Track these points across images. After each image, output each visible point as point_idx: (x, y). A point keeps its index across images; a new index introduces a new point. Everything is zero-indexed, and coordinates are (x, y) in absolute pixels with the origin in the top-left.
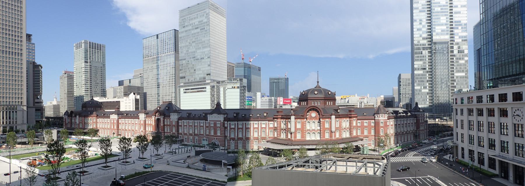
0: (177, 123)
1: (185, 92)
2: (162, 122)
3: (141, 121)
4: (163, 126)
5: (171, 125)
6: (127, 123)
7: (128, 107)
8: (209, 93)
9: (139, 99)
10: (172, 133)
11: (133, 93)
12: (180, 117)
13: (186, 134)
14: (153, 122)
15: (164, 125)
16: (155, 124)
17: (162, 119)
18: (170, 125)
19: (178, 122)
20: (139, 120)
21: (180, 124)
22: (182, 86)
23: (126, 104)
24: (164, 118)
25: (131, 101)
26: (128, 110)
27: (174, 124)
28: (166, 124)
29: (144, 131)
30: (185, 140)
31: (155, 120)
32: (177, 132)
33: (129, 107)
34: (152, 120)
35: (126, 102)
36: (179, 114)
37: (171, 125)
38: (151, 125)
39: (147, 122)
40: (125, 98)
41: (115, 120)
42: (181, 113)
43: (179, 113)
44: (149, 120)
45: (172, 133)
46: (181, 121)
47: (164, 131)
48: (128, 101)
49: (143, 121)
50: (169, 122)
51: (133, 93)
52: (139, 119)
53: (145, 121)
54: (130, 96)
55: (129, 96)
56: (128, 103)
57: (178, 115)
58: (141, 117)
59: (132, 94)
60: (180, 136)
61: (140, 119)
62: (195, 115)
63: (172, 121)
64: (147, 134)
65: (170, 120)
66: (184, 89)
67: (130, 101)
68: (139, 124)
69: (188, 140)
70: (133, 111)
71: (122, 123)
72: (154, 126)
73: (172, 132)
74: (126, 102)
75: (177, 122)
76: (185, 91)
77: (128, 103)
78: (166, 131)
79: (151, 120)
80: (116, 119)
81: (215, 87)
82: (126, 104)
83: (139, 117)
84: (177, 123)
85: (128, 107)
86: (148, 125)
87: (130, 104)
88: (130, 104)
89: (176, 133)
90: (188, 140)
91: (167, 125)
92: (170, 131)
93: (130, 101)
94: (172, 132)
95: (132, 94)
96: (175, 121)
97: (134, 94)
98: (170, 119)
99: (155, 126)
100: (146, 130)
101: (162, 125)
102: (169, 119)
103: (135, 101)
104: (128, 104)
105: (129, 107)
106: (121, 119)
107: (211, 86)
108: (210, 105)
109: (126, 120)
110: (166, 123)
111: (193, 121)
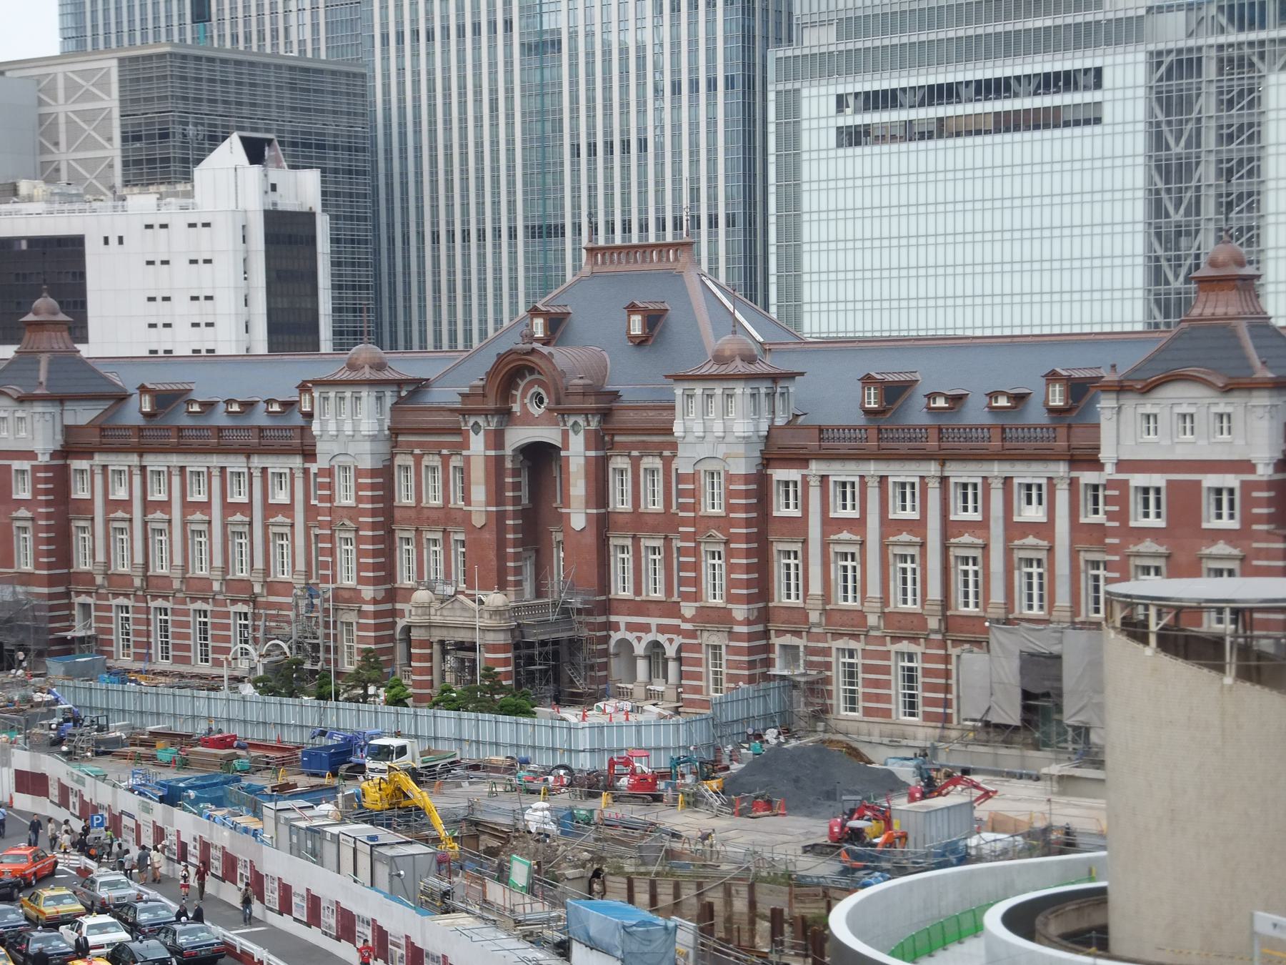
0: (747, 494)
1: (853, 137)
2: (578, 488)
3: (329, 472)
4: (590, 540)
5: (685, 521)
6: (165, 506)
7: (182, 311)
8: (1138, 143)
9: (311, 216)
10: (688, 609)
11: (235, 138)
12: (780, 422)
13: (851, 625)
14: (479, 493)
15: (603, 524)
16: (501, 516)
17: (577, 452)
18: (666, 524)
19: (760, 488)
20: (314, 468)
21: (781, 510)
22: (823, 65)
23: (159, 281)
24: (602, 442)
25: (222, 242)
26: (183, 342)
27: (712, 507)
28: (628, 507)
29: (368, 592)
30: (839, 687)
31: (499, 460)
32: (749, 599)
33: (201, 311)
34: (464, 471)
35: (158, 245)
36: (771, 396)
37: (685, 521)
38: (447, 519)
39: (404, 497)
40: (143, 202)
41: (16, 465)
42: (791, 376)
43: (774, 378)
44: (434, 461)
45: (688, 609)
46: (793, 474)
47: (604, 584)
48: (179, 242)
49: (359, 473)
50: (659, 488)
51: (235, 138)
52: (309, 454)
53: (384, 477)
54: (199, 173)
55: (187, 177)
56: (180, 264)
57: (764, 403)
58: (332, 428)
59: (231, 151)
60: (789, 640)
61: (320, 447)
62: (957, 400)
63: (693, 478)
64: (401, 623)
65: (667, 462)
66: (841, 101)
67: (203, 243)
68: (310, 511)
69: (876, 684)
70: (247, 358)
71: (111, 505)
72: (489, 536)
73: (696, 597)
74: (158, 245)
75: (747, 479)
76: (852, 119)
77: (180, 264)
78: (621, 590)
79: (456, 461)
80: (30, 455)
81: (1210, 70)
82: (159, 281)
83: (316, 427)
84: (747, 494)
85: (182, 311)
86: (421, 517)
87: (203, 279)
88: (203, 279)
89: (740, 611)
90: (876, 684)
91: (639, 523)
92: (669, 590)
93: (203, 243)
94: (696, 597)
95: (231, 151)
96: (730, 478)
97: (255, 152)
98: (674, 446)
99: (501, 529)
100: (391, 576)
101: (578, 520)
102: (657, 450)
103: (271, 239)
104: (181, 279)
105: (201, 311)
106: (99, 459)
107: (1156, 59)
108: (1137, 276)
109: (155, 462)
110: (620, 503)
111: (932, 469)
